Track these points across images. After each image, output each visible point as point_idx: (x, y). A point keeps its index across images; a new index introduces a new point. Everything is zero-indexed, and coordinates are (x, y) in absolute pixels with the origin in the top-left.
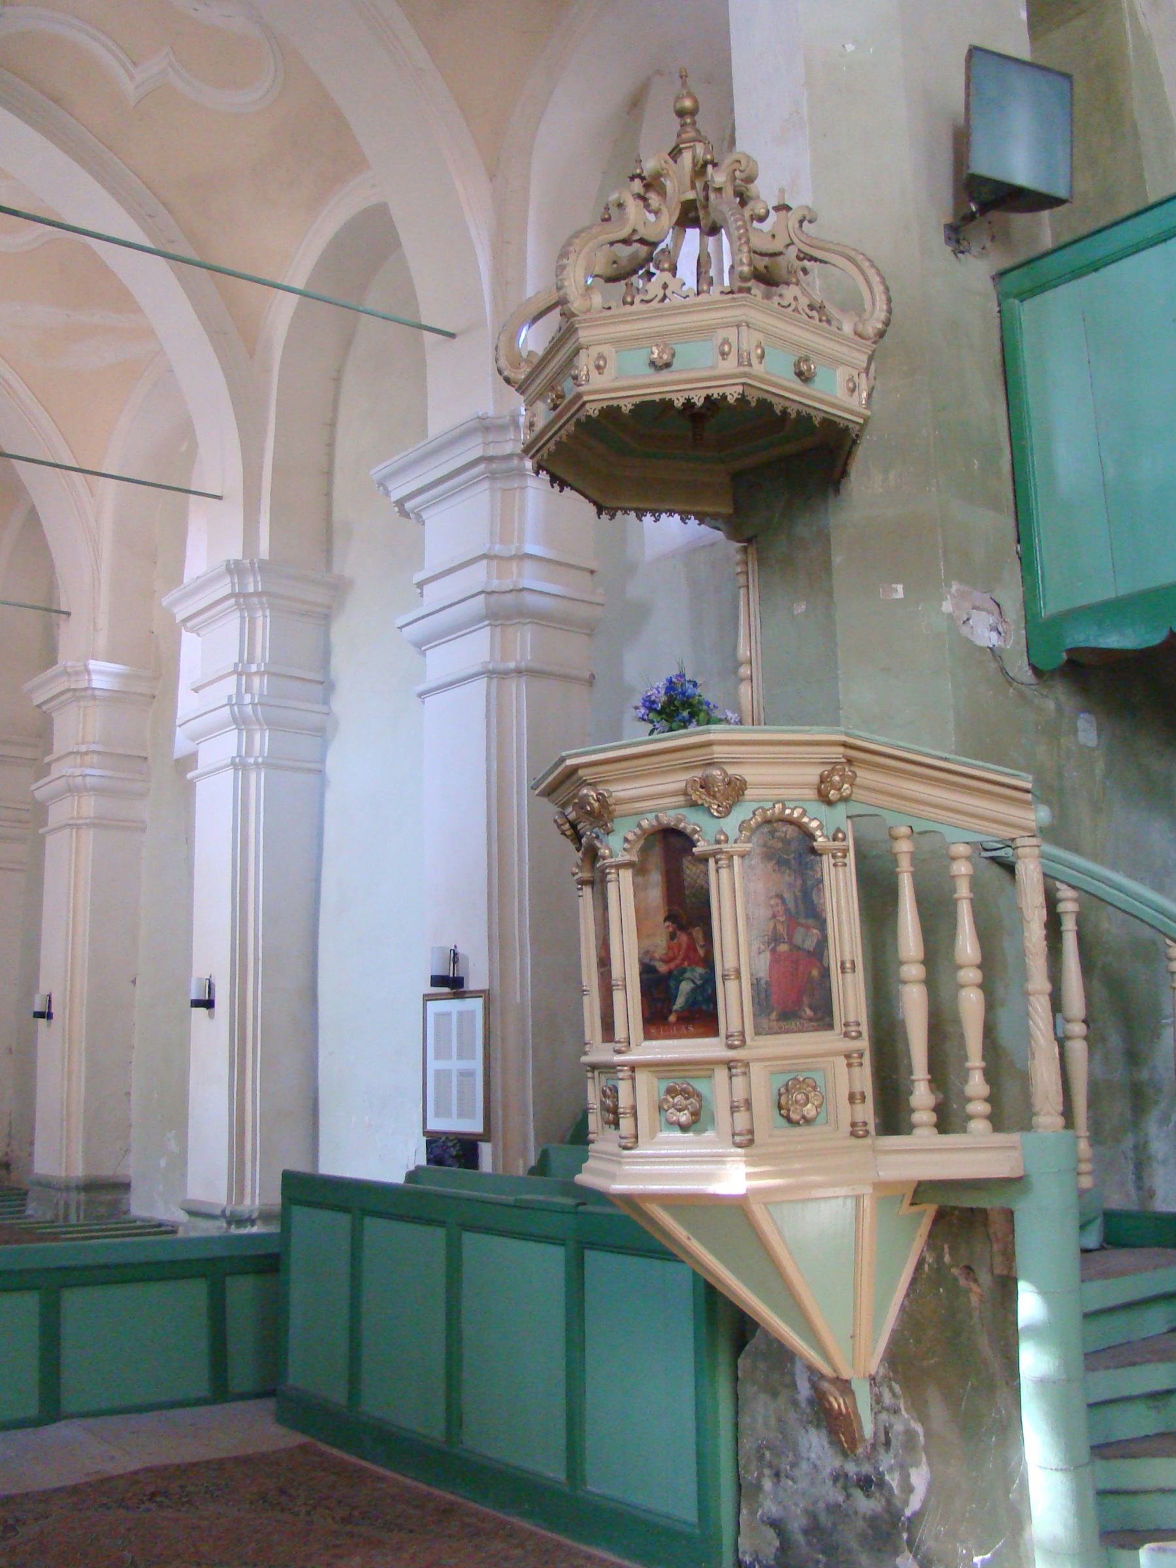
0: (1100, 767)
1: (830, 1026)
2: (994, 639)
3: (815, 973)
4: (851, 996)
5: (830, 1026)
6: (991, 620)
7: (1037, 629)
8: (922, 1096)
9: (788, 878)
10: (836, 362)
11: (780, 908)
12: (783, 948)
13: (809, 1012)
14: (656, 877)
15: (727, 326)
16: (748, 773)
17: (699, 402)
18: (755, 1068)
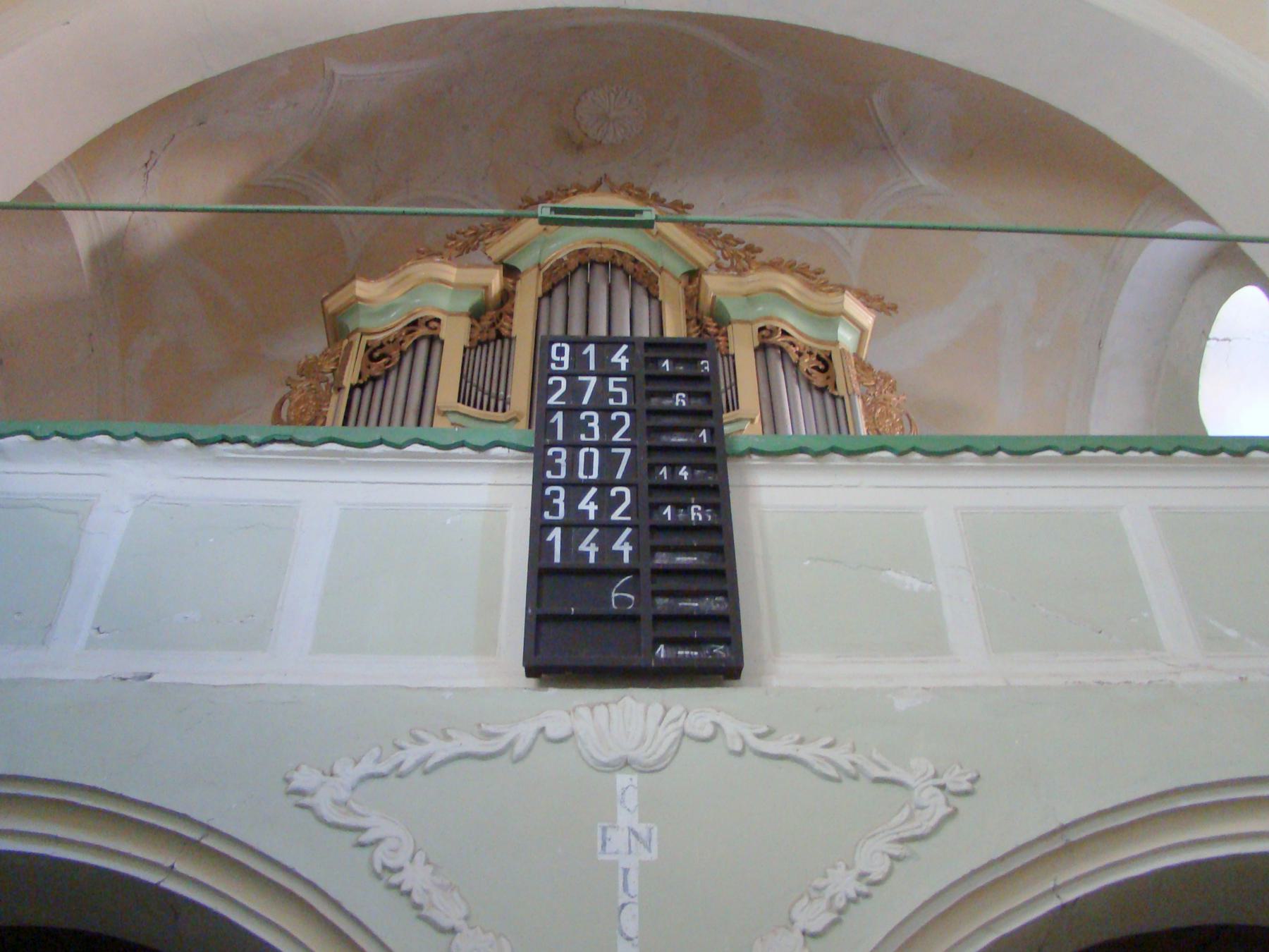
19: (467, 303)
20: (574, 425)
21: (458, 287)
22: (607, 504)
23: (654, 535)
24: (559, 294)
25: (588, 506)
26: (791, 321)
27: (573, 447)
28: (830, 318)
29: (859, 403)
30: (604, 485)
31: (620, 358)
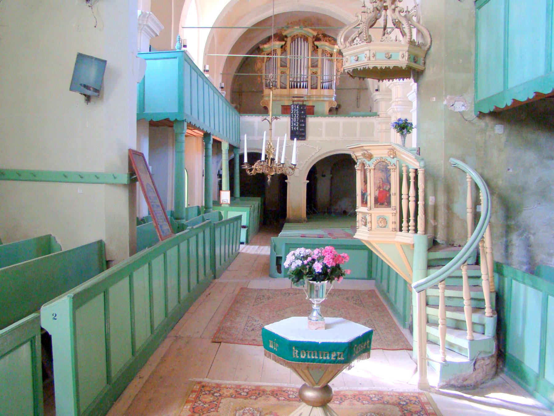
0: (504, 139)
1: (390, 207)
2: (463, 109)
4: (394, 200)
5: (390, 207)
6: (462, 103)
8: (404, 224)
12: (381, 189)
14: (363, 173)
16: (372, 152)
17: (362, 69)
18: (373, 215)
19: (280, 47)
20: (294, 115)
22: (296, 124)
23: (300, 127)
26: (327, 49)
28: (333, 49)
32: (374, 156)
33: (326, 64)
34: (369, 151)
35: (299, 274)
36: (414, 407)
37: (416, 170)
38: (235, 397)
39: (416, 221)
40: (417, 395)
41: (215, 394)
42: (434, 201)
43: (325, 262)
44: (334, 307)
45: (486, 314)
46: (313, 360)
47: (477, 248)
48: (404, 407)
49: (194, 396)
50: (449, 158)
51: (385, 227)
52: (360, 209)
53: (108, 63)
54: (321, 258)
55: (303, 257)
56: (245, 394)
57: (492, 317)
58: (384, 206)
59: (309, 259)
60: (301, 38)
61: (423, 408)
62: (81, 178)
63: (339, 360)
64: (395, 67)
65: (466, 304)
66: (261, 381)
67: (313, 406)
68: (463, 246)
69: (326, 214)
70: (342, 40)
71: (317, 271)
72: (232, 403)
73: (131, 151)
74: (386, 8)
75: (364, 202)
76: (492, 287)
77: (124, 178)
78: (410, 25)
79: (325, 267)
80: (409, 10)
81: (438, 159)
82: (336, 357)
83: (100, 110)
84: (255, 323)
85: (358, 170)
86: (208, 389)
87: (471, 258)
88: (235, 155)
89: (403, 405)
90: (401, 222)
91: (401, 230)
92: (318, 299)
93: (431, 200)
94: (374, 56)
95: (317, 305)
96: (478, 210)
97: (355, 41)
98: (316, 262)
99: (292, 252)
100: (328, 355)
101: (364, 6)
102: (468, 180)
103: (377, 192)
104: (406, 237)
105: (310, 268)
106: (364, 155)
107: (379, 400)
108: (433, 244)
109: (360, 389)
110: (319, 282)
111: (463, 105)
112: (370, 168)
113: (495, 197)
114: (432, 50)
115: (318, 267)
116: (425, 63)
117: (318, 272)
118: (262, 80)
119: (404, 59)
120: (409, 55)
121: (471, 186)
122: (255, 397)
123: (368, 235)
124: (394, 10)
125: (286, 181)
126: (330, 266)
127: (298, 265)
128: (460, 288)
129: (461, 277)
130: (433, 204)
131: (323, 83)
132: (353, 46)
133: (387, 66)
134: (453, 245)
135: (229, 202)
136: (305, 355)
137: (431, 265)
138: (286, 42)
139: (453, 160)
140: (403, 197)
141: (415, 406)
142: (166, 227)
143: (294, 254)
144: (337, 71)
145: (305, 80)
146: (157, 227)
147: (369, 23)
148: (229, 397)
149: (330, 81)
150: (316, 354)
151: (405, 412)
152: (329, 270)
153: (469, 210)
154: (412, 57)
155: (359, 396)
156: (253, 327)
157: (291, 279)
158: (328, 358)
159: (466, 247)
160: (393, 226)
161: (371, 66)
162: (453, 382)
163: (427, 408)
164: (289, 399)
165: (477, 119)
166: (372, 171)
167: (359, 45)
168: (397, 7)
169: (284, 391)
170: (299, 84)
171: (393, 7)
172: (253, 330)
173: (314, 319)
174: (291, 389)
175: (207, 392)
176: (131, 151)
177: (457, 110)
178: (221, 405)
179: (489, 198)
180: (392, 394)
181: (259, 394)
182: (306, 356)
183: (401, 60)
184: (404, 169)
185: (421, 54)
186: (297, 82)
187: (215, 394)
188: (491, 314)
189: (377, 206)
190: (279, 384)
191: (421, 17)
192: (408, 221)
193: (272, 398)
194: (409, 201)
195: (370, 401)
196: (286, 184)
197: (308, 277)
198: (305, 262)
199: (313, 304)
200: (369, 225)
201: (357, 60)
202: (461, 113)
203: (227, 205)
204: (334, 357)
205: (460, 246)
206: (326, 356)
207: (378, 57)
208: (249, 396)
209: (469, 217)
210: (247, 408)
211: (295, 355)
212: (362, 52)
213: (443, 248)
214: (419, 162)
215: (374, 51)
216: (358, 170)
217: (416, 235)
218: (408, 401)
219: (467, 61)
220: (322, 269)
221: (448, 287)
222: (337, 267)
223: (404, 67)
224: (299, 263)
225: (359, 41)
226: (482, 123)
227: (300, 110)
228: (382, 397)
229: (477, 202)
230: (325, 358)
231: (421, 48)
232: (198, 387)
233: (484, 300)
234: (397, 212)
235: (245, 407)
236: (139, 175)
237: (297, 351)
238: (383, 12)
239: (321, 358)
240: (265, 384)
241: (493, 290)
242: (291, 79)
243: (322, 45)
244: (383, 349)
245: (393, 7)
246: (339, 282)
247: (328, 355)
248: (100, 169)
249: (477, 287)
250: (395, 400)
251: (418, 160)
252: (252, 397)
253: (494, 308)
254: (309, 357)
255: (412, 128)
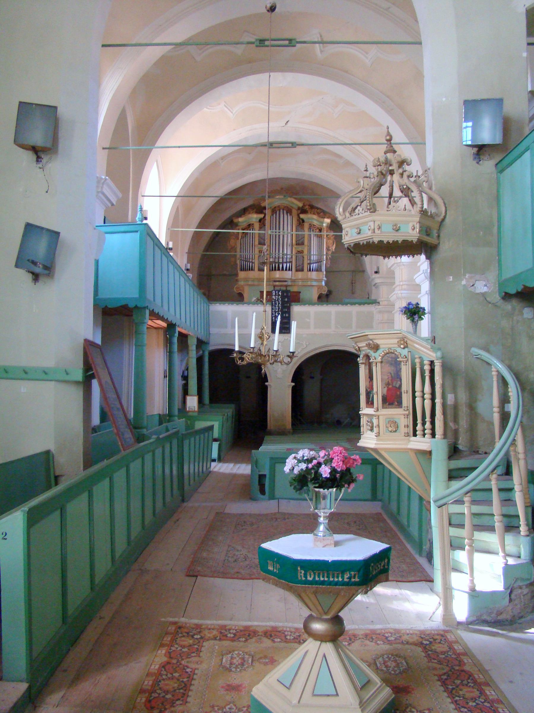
1: (401, 407)
2: (485, 289)
3: (398, 393)
4: (406, 399)
5: (401, 407)
7: (501, 284)
8: (419, 427)
9: (393, 368)
10: (407, 222)
11: (390, 376)
12: (390, 386)
13: (396, 403)
14: (367, 367)
15: (370, 221)
17: (365, 243)
19: (258, 221)
20: (276, 304)
21: (256, 218)
24: (274, 215)
25: (277, 314)
26: (315, 223)
27: (275, 306)
28: (322, 223)
29: (325, 240)
30: (278, 311)
31: (280, 293)
32: (381, 346)
33: (314, 242)
34: (375, 341)
35: (302, 481)
36: (439, 647)
37: (432, 363)
38: (220, 640)
39: (433, 423)
40: (442, 633)
41: (195, 637)
42: (453, 400)
43: (334, 465)
44: (340, 524)
45: (522, 533)
46: (323, 583)
47: (507, 454)
48: (427, 647)
49: (169, 639)
50: (471, 347)
51: (396, 431)
52: (365, 410)
53: (61, 234)
54: (329, 461)
55: (307, 460)
56: (232, 635)
57: (528, 536)
58: (394, 406)
59: (315, 462)
60: (283, 210)
61: (451, 648)
62: (25, 374)
63: (353, 582)
64: (404, 241)
65: (498, 522)
66: (250, 620)
67: (322, 641)
68: (489, 454)
69: (316, 425)
70: (341, 210)
71: (324, 476)
72: (217, 647)
73: (86, 341)
74: (392, 173)
75: (370, 403)
76: (528, 501)
77: (78, 375)
78: (421, 192)
79: (334, 471)
80: (419, 174)
81: (457, 350)
82: (350, 578)
83: (50, 292)
84: (237, 553)
85: (362, 363)
86: (186, 630)
87: (501, 467)
88: (203, 352)
89: (427, 644)
90: (415, 424)
91: (415, 435)
92: (326, 511)
93: (450, 398)
94: (379, 228)
95: (324, 517)
96: (506, 410)
97: (357, 211)
98: (323, 466)
99: (293, 455)
100: (340, 575)
101: (366, 170)
102: (494, 373)
103: (386, 389)
104: (421, 443)
105: (316, 473)
106: (368, 345)
107: (396, 639)
108: (454, 452)
109: (372, 627)
110: (326, 490)
111: (485, 285)
112: (377, 360)
113: (526, 394)
114: (447, 220)
115: (325, 471)
116: (439, 236)
117: (326, 478)
118: (235, 262)
119: (415, 232)
120: (420, 227)
121: (498, 381)
122: (244, 639)
123: (375, 442)
124: (402, 175)
125: (266, 384)
126: (339, 470)
127: (302, 469)
128: (489, 503)
129: (491, 490)
130: (452, 403)
131: (310, 264)
132: (354, 217)
133: (396, 240)
134: (478, 452)
135: (196, 409)
136: (312, 576)
137: (453, 475)
138: (265, 214)
139: (475, 351)
140: (417, 394)
141: (440, 645)
142: (128, 435)
143: (295, 458)
144: (328, 249)
145: (288, 260)
146: (118, 434)
147: (373, 189)
148: (212, 639)
149: (319, 261)
150: (326, 574)
151: (430, 652)
152: (338, 475)
153: (496, 410)
154: (424, 229)
155: (371, 636)
156: (235, 558)
157: (293, 487)
158: (340, 579)
159: (495, 451)
160: (406, 430)
161: (376, 240)
162: (485, 617)
163: (456, 647)
164: (286, 641)
165: (502, 301)
166: (379, 365)
167: (361, 215)
168: (405, 171)
169: (279, 632)
170: (281, 266)
171: (401, 171)
172: (235, 561)
173: (321, 534)
174: (288, 629)
175: (185, 634)
176: (86, 341)
177: (478, 291)
178: (203, 649)
179: (520, 394)
180: (411, 632)
181: (249, 636)
182: (314, 578)
183: (411, 232)
184: (417, 361)
185: (435, 226)
186: (279, 263)
187: (195, 637)
188: (528, 533)
189: (385, 406)
190: (272, 624)
191: (433, 182)
192: (424, 424)
193: (265, 640)
194: (424, 399)
195: (386, 641)
196: (266, 388)
197: (314, 483)
198: (310, 466)
199: (320, 516)
200: (376, 430)
201: (359, 233)
202: (484, 295)
203: (196, 414)
204: (347, 578)
205: (486, 453)
206: (338, 577)
207: (384, 229)
208: (236, 637)
209: (496, 418)
210: (236, 652)
211: (301, 576)
212: (366, 223)
213: (466, 456)
214: (436, 353)
215: (379, 223)
216: (362, 363)
217: (434, 439)
218: (431, 640)
219: (489, 234)
220: (330, 473)
221: (474, 502)
222: (348, 470)
223: (415, 240)
224: (303, 466)
225: (361, 211)
226: (508, 306)
227: (283, 297)
228: (400, 637)
229: (505, 400)
230: (336, 579)
231: (434, 218)
232: (174, 628)
233: (518, 516)
234: (409, 413)
235: (234, 651)
236: (97, 371)
237: (303, 572)
238: (389, 178)
239: (331, 579)
240: (256, 623)
241: (529, 504)
242: (271, 260)
243: (309, 219)
244: (397, 581)
245: (401, 171)
246: (349, 490)
247: (340, 575)
248: (49, 362)
249: (508, 501)
250: (415, 639)
251: (433, 349)
252: (241, 639)
253: (531, 527)
254: (317, 579)
255: (425, 314)
